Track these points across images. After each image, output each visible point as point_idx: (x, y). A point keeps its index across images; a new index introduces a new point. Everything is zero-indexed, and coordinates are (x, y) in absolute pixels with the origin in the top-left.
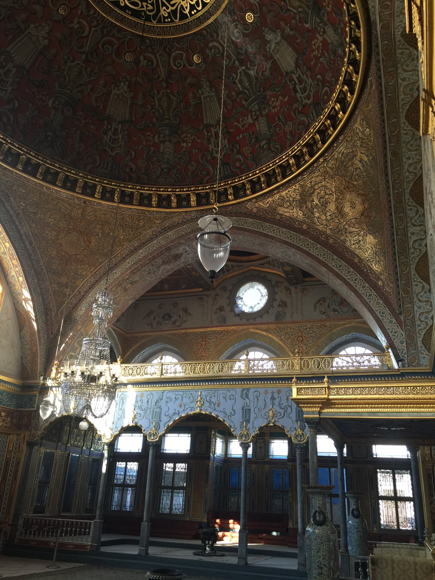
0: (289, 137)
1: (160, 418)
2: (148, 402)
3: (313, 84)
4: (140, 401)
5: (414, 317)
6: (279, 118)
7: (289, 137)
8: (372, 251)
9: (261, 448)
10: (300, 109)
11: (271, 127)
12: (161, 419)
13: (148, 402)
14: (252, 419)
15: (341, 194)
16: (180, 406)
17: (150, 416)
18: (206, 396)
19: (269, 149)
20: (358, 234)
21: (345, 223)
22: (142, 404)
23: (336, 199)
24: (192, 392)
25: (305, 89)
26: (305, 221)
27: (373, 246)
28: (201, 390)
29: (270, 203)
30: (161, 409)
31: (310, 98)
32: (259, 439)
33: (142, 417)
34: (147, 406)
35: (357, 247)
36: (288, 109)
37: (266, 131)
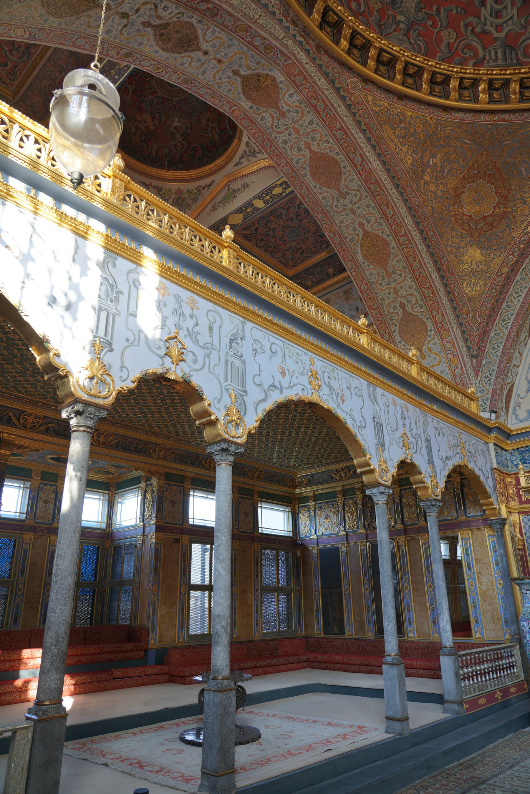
0: (443, 47)
1: (243, 385)
2: (211, 329)
3: (515, 18)
4: (191, 317)
5: (509, 367)
6: (438, 10)
7: (443, 47)
8: (469, 267)
9: (46, 502)
10: (477, 30)
11: (421, 11)
12: (247, 389)
13: (211, 329)
14: (387, 444)
15: (474, 176)
16: (283, 374)
17: (220, 370)
18: (323, 373)
19: (407, 35)
20: (462, 237)
21: (454, 213)
22: (196, 329)
23: (464, 177)
24: (300, 352)
25: (498, 14)
26: (409, 174)
27: (474, 262)
28: (314, 356)
29: (382, 108)
30: (243, 362)
31: (501, 31)
32: (46, 485)
33: (199, 365)
34: (210, 340)
35: (454, 251)
36: (457, 13)
37: (412, 7)
